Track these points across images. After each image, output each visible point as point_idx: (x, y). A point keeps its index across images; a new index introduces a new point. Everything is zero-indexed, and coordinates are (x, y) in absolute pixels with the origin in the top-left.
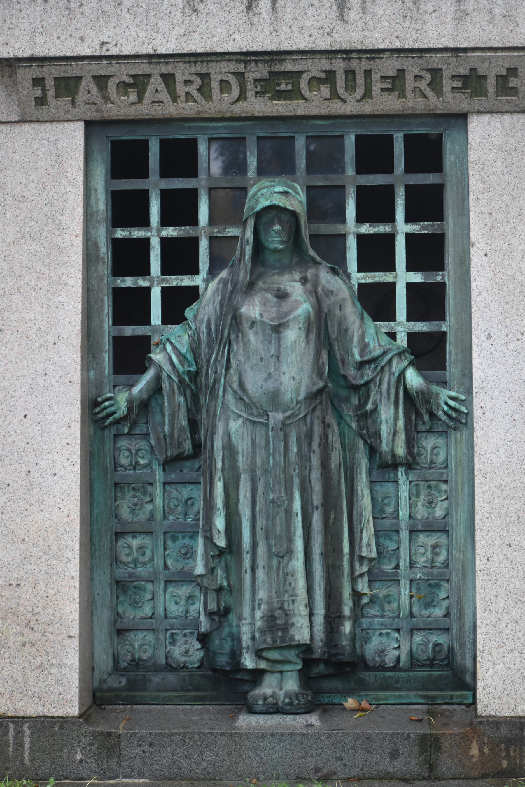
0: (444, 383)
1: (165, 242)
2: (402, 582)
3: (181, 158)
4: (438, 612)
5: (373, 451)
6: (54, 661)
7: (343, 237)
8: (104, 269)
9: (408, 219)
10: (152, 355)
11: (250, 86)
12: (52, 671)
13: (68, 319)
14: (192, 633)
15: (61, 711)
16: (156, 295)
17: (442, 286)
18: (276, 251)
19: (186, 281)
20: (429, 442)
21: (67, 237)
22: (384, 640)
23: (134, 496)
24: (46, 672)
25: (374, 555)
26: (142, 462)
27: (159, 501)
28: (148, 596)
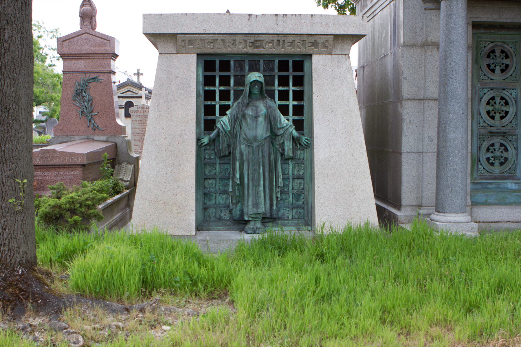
0: (303, 135)
1: (220, 91)
3: (225, 65)
4: (300, 203)
5: (282, 155)
7: (274, 90)
8: (202, 99)
9: (293, 86)
10: (217, 125)
11: (248, 43)
16: (217, 107)
17: (303, 105)
18: (255, 94)
19: (227, 103)
20: (299, 152)
22: (284, 211)
25: (282, 186)
26: (212, 157)
27: (217, 169)
28: (214, 198)
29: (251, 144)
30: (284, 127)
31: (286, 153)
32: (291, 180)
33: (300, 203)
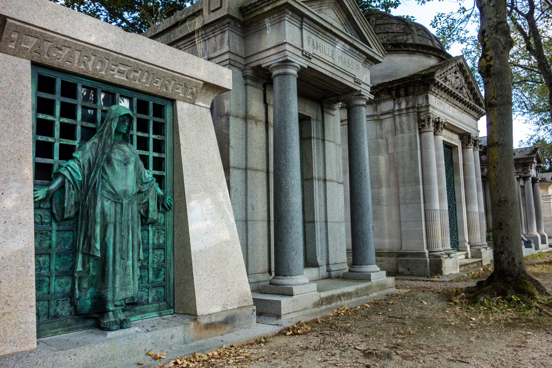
1: (62, 124)
2: (150, 269)
4: (160, 280)
6: (22, 321)
12: (21, 326)
13: (25, 149)
14: (67, 299)
15: (27, 347)
16: (57, 146)
19: (71, 142)
21: (24, 110)
22: (142, 292)
23: (41, 237)
24: (18, 327)
28: (46, 284)
29: (119, 199)
30: (149, 182)
31: (150, 216)
32: (151, 250)
33: (160, 280)
